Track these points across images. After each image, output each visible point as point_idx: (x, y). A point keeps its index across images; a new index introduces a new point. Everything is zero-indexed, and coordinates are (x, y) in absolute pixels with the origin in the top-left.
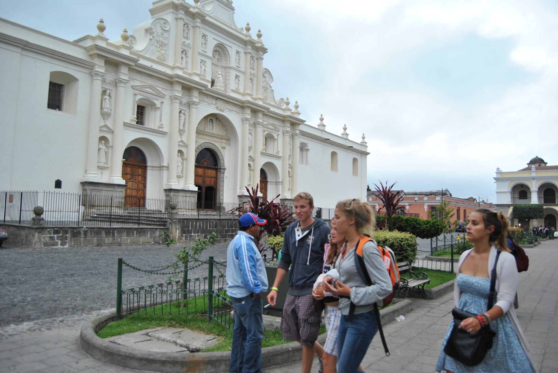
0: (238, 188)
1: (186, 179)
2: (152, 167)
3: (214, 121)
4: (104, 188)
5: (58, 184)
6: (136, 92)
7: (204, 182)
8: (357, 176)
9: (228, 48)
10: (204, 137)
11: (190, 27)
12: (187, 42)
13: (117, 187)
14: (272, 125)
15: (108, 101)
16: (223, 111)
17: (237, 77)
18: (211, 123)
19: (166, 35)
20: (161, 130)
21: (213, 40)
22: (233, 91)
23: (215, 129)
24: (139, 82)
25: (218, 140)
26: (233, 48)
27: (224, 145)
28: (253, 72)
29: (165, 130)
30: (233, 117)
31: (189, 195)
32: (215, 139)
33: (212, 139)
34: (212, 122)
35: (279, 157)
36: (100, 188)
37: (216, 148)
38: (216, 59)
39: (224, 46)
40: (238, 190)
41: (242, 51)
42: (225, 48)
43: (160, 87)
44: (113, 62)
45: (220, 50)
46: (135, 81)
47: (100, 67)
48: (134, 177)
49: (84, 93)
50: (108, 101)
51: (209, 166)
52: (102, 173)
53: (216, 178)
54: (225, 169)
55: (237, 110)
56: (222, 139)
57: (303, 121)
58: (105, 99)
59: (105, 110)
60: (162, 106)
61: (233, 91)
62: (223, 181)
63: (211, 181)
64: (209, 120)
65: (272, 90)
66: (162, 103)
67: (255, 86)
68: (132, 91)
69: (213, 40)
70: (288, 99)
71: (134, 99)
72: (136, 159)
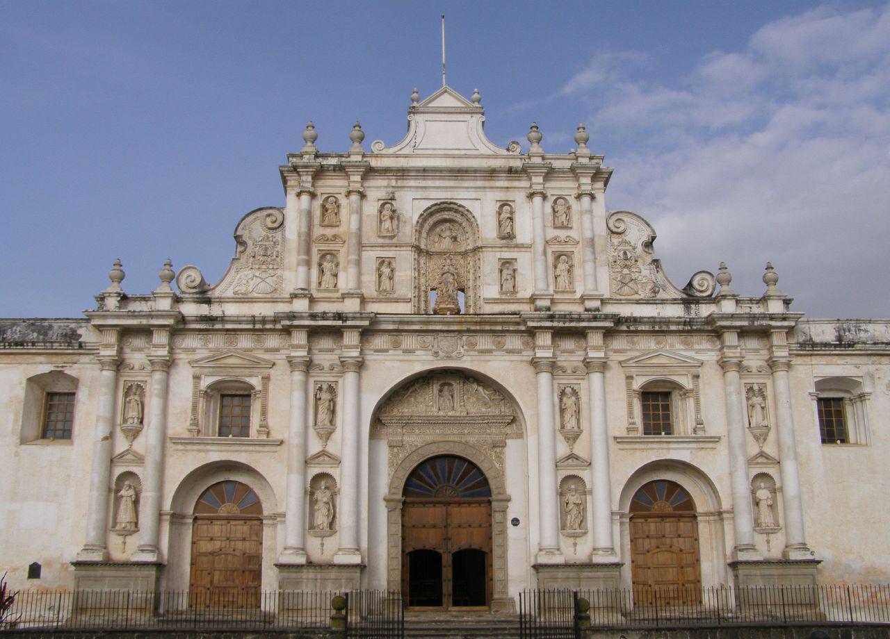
5: (35, 571)
13: (135, 568)
15: (133, 404)
16: (459, 358)
17: (506, 263)
19: (278, 235)
22: (488, 301)
23: (469, 403)
28: (562, 234)
29: (276, 435)
30: (501, 365)
41: (519, 198)
42: (460, 206)
50: (133, 404)
54: (509, 500)
55: (514, 342)
58: (129, 402)
59: (130, 421)
60: (265, 386)
62: (503, 532)
66: (266, 379)
69: (412, 204)
71: (196, 386)
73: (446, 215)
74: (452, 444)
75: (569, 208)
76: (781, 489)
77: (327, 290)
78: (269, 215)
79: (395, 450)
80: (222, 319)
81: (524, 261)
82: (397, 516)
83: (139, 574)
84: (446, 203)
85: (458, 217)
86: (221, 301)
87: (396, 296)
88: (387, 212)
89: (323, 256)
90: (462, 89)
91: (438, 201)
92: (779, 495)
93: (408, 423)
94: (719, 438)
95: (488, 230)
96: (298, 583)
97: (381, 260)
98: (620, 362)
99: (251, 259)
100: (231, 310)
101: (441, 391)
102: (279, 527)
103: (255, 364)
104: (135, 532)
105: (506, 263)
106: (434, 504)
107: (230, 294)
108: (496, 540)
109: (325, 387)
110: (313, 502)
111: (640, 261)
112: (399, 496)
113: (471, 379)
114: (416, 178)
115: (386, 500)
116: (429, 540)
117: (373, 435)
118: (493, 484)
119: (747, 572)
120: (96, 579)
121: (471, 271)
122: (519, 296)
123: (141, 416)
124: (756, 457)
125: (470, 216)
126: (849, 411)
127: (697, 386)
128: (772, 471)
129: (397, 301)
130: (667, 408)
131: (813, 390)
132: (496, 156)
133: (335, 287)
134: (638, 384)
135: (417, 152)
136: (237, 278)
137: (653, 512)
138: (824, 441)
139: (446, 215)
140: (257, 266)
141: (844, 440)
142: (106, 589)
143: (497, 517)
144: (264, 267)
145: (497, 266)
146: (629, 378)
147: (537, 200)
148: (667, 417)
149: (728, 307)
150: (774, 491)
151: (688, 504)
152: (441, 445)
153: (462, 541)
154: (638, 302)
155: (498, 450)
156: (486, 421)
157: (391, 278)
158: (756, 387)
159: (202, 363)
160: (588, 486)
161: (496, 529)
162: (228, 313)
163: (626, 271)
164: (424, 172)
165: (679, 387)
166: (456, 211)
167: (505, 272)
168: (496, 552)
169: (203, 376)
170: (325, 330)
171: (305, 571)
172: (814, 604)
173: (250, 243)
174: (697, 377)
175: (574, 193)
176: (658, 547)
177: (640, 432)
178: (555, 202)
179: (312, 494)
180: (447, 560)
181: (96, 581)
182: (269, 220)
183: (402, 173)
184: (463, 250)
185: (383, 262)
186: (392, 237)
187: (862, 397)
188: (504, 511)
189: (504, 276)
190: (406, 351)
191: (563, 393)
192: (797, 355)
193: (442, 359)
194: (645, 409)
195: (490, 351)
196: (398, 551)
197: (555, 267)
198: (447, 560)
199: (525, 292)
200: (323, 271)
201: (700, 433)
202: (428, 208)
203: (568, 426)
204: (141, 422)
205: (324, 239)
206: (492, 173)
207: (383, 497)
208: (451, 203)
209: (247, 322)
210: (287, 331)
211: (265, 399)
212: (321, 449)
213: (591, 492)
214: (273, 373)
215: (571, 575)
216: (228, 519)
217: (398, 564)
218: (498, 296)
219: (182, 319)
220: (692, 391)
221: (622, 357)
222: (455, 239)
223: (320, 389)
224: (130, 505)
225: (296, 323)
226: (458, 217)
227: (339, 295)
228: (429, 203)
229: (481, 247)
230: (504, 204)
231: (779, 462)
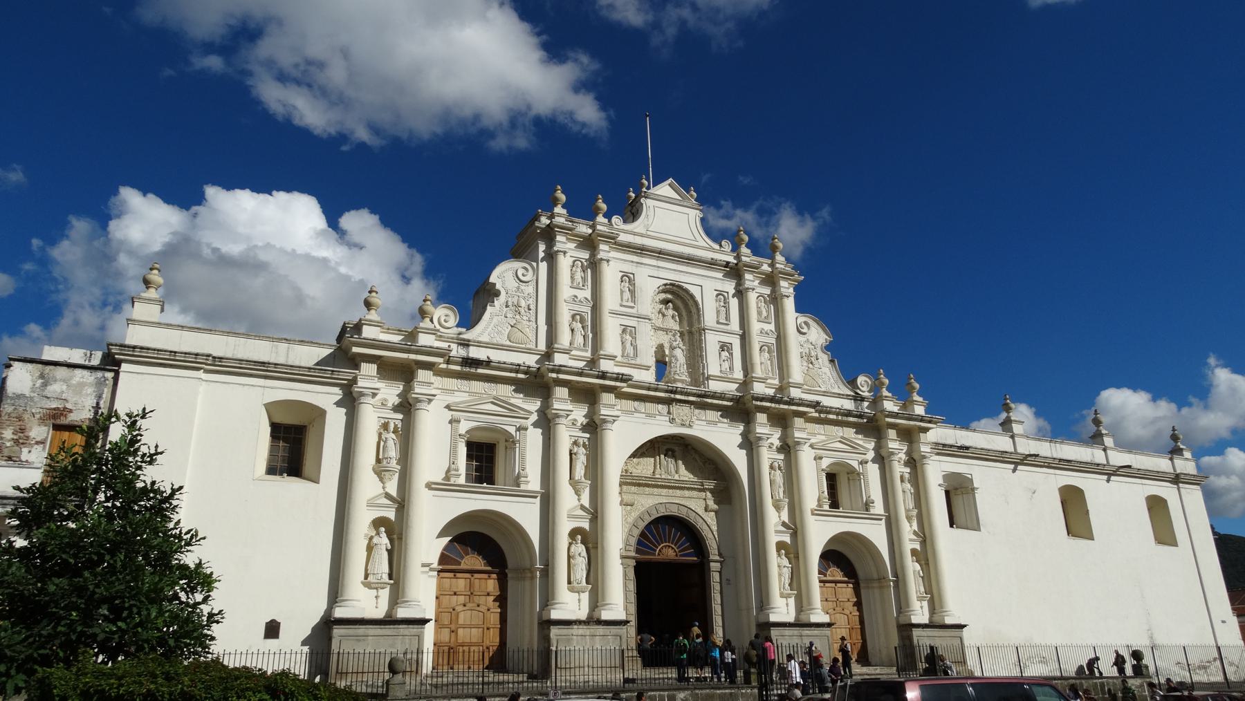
5: (272, 630)
8: (1173, 542)
16: (690, 426)
20: (523, 487)
25: (695, 493)
30: (724, 437)
32: (687, 493)
33: (678, 492)
36: (361, 630)
37: (692, 515)
42: (686, 291)
68: (448, 415)
69: (650, 279)
80: (487, 364)
86: (480, 344)
87: (638, 361)
90: (684, 183)
95: (709, 316)
100: (496, 356)
107: (485, 338)
112: (633, 554)
115: (623, 557)
132: (712, 250)
134: (825, 463)
142: (369, 649)
159: (462, 407)
164: (660, 254)
172: (965, 662)
173: (503, 293)
177: (826, 507)
183: (641, 250)
190: (649, 415)
192: (938, 454)
195: (715, 423)
206: (711, 264)
209: (511, 371)
221: (813, 441)
224: (385, 555)
225: (562, 376)
230: (720, 293)
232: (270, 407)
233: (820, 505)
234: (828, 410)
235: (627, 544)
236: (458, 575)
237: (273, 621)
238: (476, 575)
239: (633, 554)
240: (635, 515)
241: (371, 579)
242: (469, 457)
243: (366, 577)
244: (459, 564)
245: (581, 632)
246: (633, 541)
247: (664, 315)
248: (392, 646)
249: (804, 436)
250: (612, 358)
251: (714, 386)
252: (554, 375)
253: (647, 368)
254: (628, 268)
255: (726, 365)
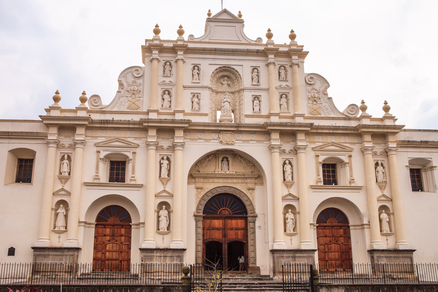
0: (270, 239)
1: (186, 237)
2: (355, 226)
3: (230, 159)
4: (51, 253)
5: (11, 252)
6: (99, 149)
7: (225, 236)
9: (236, 68)
10: (216, 180)
11: (173, 63)
12: (167, 80)
14: (333, 144)
15: (65, 165)
16: (232, 144)
17: (256, 98)
18: (225, 162)
19: (140, 81)
21: (209, 66)
22: (247, 116)
24: (104, 138)
25: (240, 181)
26: (244, 67)
27: (250, 186)
28: (284, 84)
29: (139, 182)
30: (254, 148)
31: (169, 254)
32: (235, 181)
33: (230, 181)
34: (228, 161)
35: (359, 188)
36: (46, 253)
38: (226, 85)
39: (230, 68)
40: (270, 244)
42: (233, 69)
43: (131, 137)
44: (67, 127)
45: (227, 74)
46: (99, 138)
47: (53, 134)
48: (115, 238)
49: (46, 163)
50: (65, 165)
51: (231, 215)
52: (59, 237)
53: (246, 229)
54: (256, 216)
56: (246, 178)
57: (400, 128)
58: (63, 164)
60: (134, 157)
61: (247, 116)
62: (254, 233)
63: (237, 234)
64: (221, 159)
65: (330, 98)
66: (134, 153)
67: (291, 102)
68: (96, 149)
69: (209, 66)
70: (363, 102)
71: (98, 156)
72: (114, 219)
73: (225, 73)
74: (228, 188)
75: (286, 71)
76: (393, 214)
77: (166, 108)
78: (137, 70)
79: (200, 190)
80: (113, 122)
81: (264, 96)
82: (200, 224)
83: (68, 253)
84: (226, 67)
85: (232, 76)
88: (196, 71)
89: (164, 93)
91: (222, 66)
92: (392, 216)
93: (206, 177)
94: (362, 187)
96: (151, 258)
97: (193, 94)
98: (313, 149)
99: (127, 92)
100: (117, 117)
101: (222, 161)
102: (141, 229)
103: (130, 145)
104: (64, 232)
105: (256, 98)
106: (217, 218)
108: (250, 237)
109: (165, 158)
110: (159, 217)
111: (322, 99)
112: (201, 214)
113: (237, 155)
114: (211, 54)
115: (195, 216)
116: (217, 236)
117: (189, 183)
118: (248, 208)
119: (378, 255)
120: (45, 256)
121: (238, 101)
122: (262, 114)
123: (69, 171)
124: (380, 197)
125: (237, 74)
126: (424, 175)
127: (350, 161)
128: (388, 204)
129: (202, 115)
130: (334, 172)
131: (408, 164)
133: (170, 107)
134: (321, 159)
135: (210, 41)
136: (119, 102)
137: (328, 224)
138: (413, 190)
139: (225, 73)
140: (130, 96)
141: (422, 190)
142: (50, 262)
143: (250, 225)
144: (133, 96)
145: (251, 99)
146: (318, 156)
147: (272, 66)
148: (334, 176)
149: (366, 122)
150: (389, 215)
151: (345, 220)
152: (223, 188)
153: (232, 236)
154: (322, 118)
155: (251, 191)
156: (244, 177)
157: (198, 104)
158: (380, 162)
160: (297, 210)
161: (250, 231)
162: (115, 119)
163: (315, 103)
165: (342, 162)
166: (230, 72)
167: (255, 102)
168: (250, 242)
169: (101, 151)
170: (166, 130)
171: (155, 252)
174: (350, 156)
175: (289, 64)
176: (331, 242)
177: (322, 184)
178: (280, 68)
179: (158, 212)
180: (225, 247)
181: (45, 257)
182: (137, 72)
184: (233, 90)
185: (194, 96)
186: (199, 83)
187: (432, 168)
188: (254, 222)
189: (255, 104)
190: (206, 140)
191: (284, 163)
192: (401, 147)
193: (224, 145)
194: (324, 171)
196: (200, 242)
197: (280, 101)
198: (225, 247)
199: (264, 112)
200: (164, 99)
201: (353, 185)
202: (217, 69)
203: (287, 180)
204: (69, 174)
205: (164, 83)
207: (193, 214)
208: (228, 67)
210: (145, 130)
211: (134, 163)
212: (163, 189)
213: (299, 213)
214: (138, 151)
215: (291, 255)
216: (113, 226)
217: (200, 248)
218: (252, 114)
219: (92, 122)
220: (348, 163)
221: (313, 146)
222: (229, 85)
223: (163, 159)
226: (232, 76)
227: (172, 111)
228: (217, 67)
229: (243, 90)
231: (392, 200)
232: (13, 152)
233: (317, 182)
234: (318, 128)
235: (198, 209)
236: (106, 227)
237: (12, 248)
238: (115, 227)
239: (201, 214)
240: (203, 193)
241: (57, 229)
242: (112, 169)
243: (55, 227)
244: (107, 221)
245: (158, 254)
246: (202, 208)
247: (222, 84)
248: (61, 260)
249: (304, 144)
250: (183, 112)
251: (248, 121)
252: (146, 124)
253: (206, 115)
254: (196, 62)
255: (257, 109)
